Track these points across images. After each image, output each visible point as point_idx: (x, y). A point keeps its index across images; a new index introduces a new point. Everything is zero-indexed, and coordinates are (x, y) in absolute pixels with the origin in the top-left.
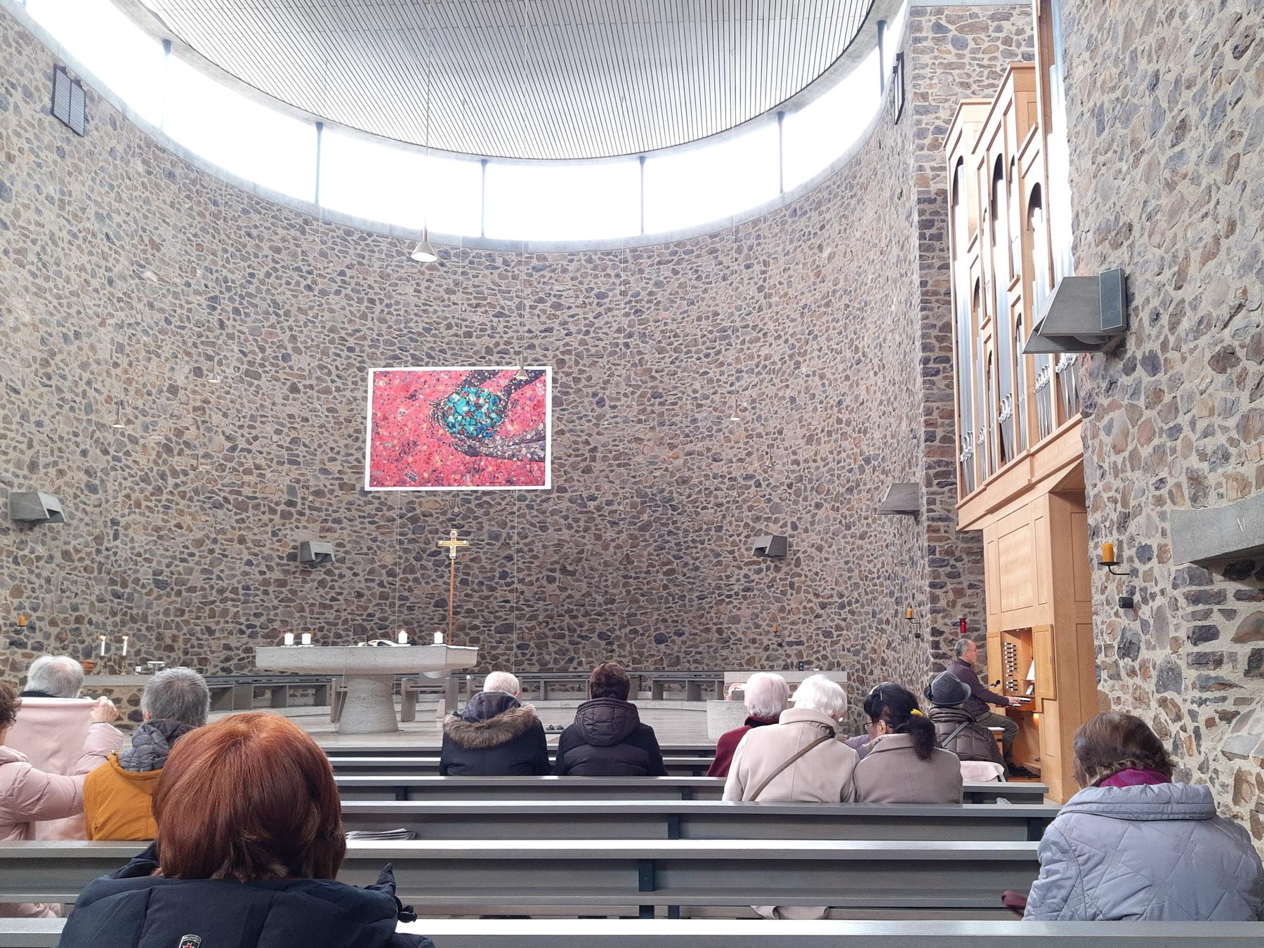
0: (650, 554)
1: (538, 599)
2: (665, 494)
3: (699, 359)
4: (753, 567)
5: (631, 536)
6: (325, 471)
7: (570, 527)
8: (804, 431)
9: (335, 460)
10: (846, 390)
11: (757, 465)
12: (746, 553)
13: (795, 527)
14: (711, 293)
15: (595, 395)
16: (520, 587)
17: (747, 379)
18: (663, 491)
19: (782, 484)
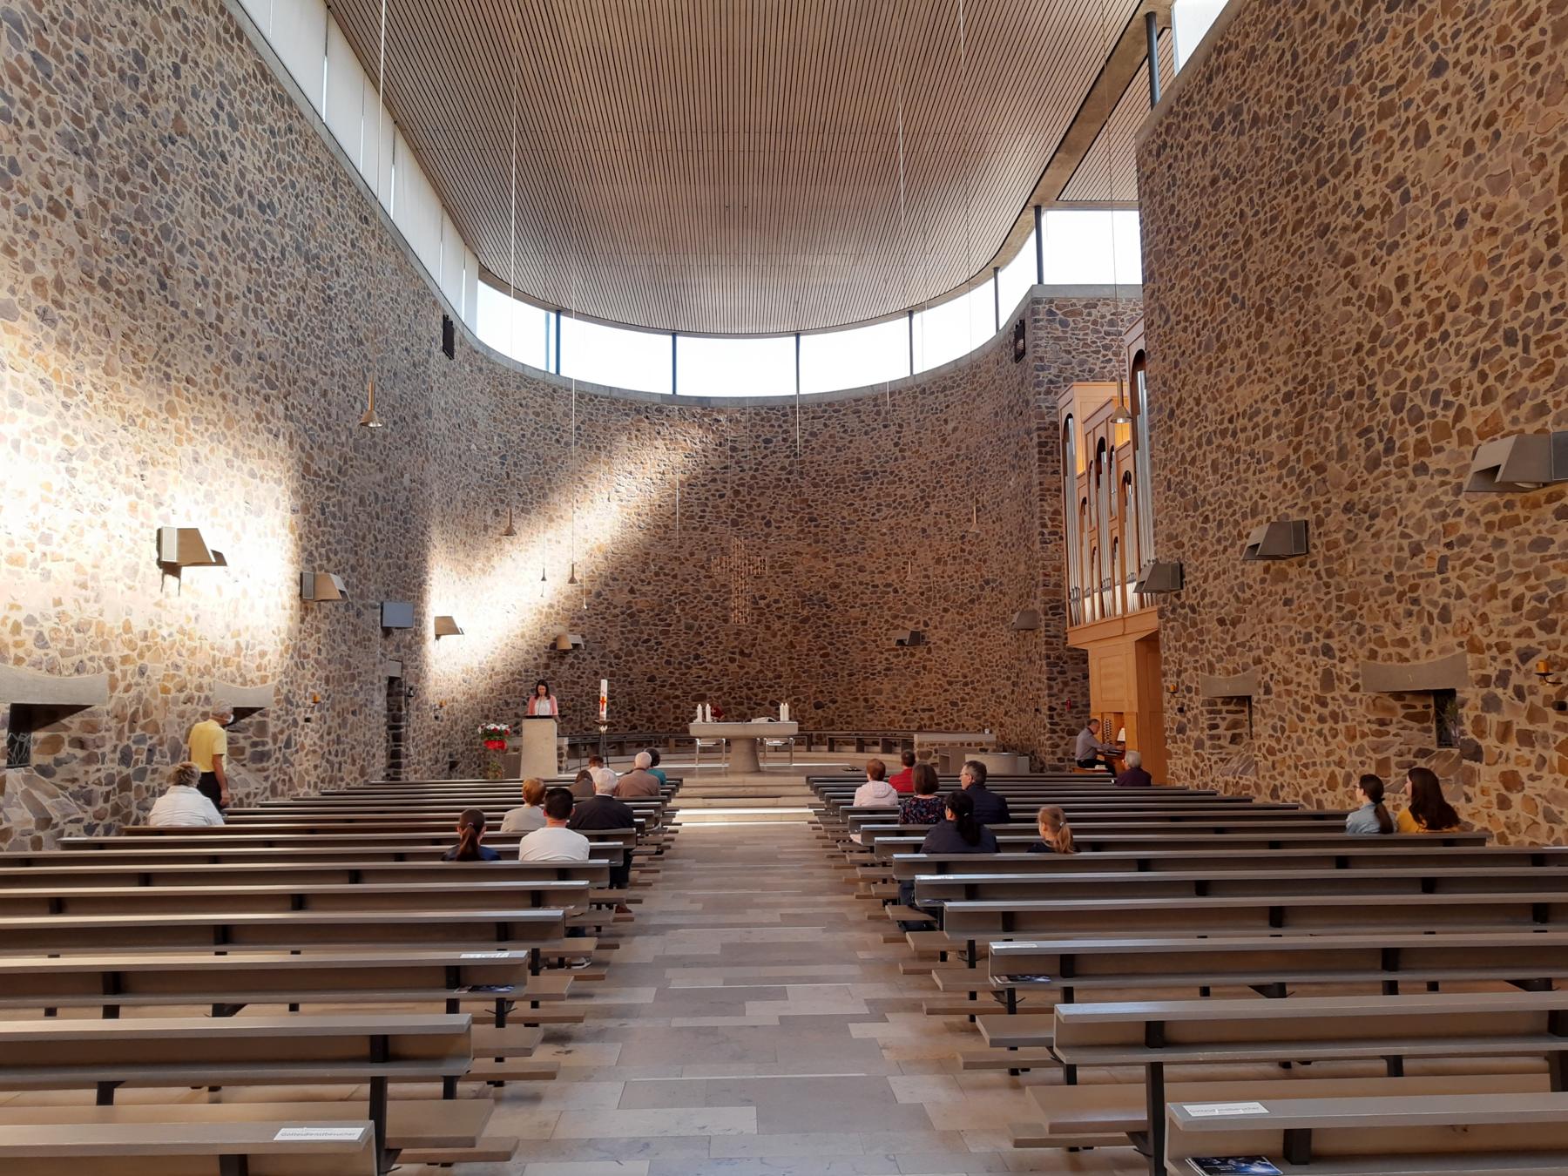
5: (794, 627)
13: (926, 625)
14: (856, 444)
16: (709, 666)
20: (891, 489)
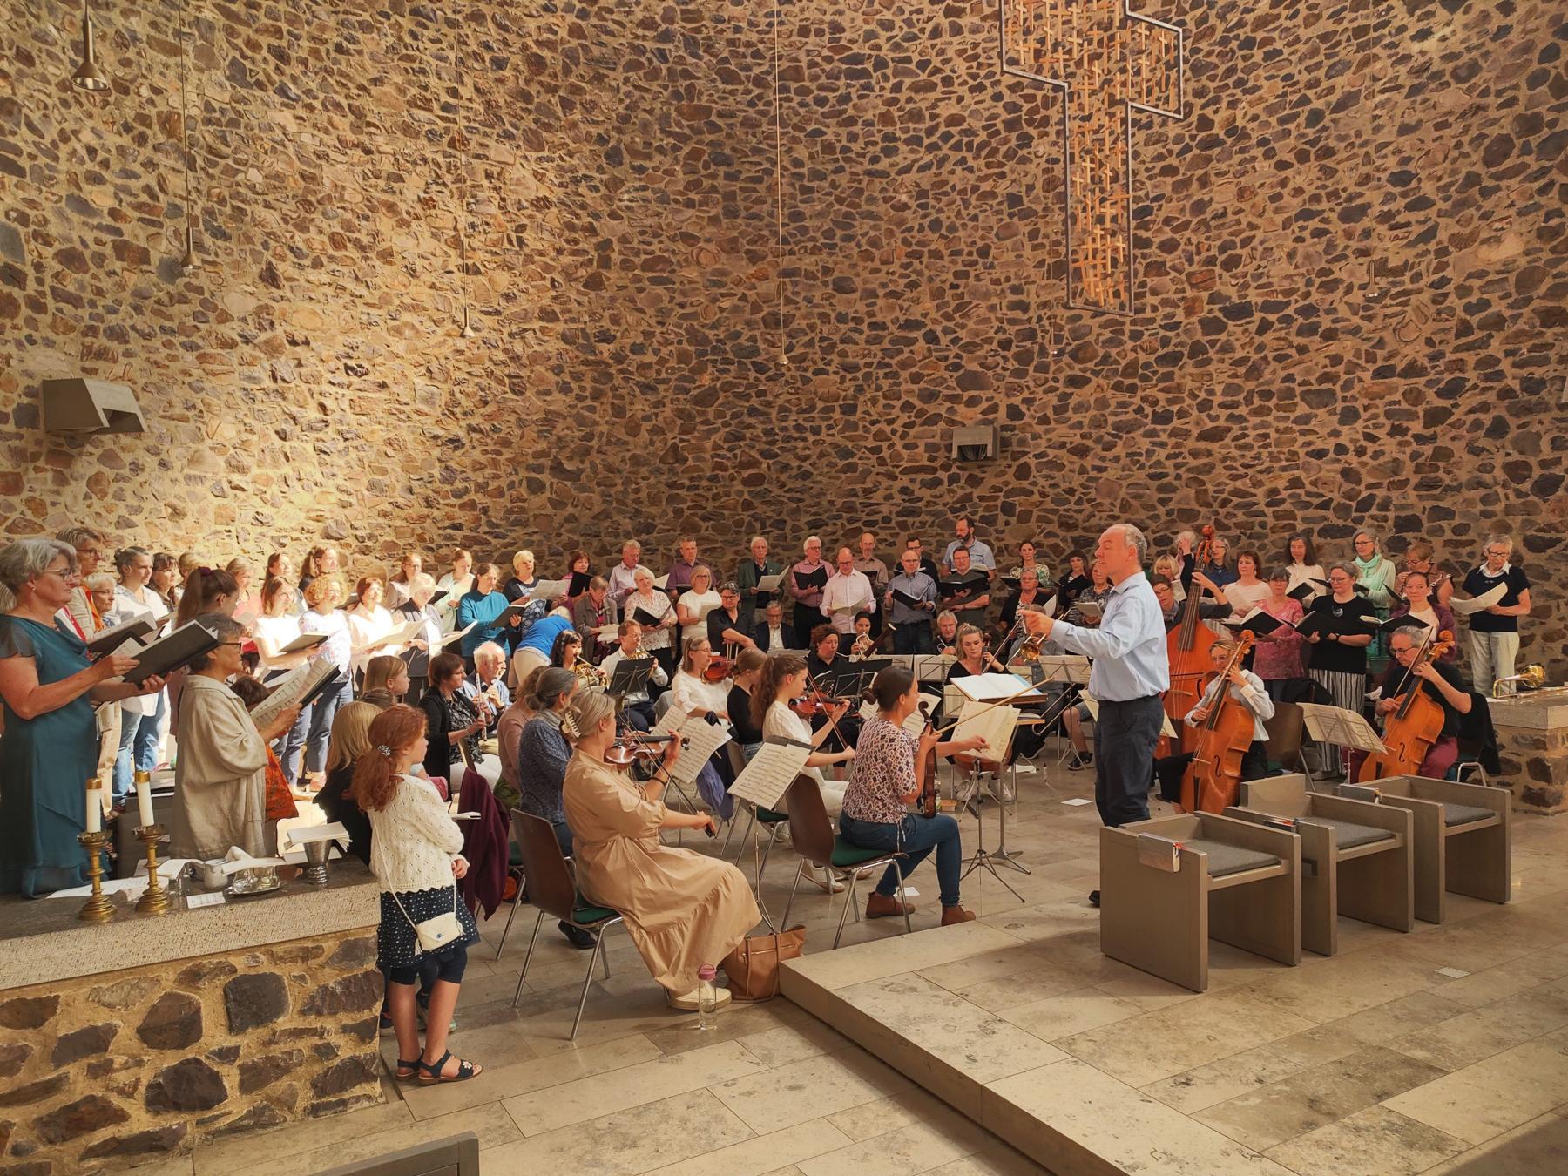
0: (716, 447)
1: (513, 524)
2: (743, 340)
3: (802, 104)
4: (920, 477)
5: (680, 413)
6: (83, 207)
7: (565, 389)
8: (1041, 255)
9: (96, 179)
10: (1168, 190)
11: (929, 304)
12: (905, 453)
15: (602, 140)
16: (479, 498)
17: (904, 155)
18: (738, 335)
19: (989, 341)
20: (923, 102)
